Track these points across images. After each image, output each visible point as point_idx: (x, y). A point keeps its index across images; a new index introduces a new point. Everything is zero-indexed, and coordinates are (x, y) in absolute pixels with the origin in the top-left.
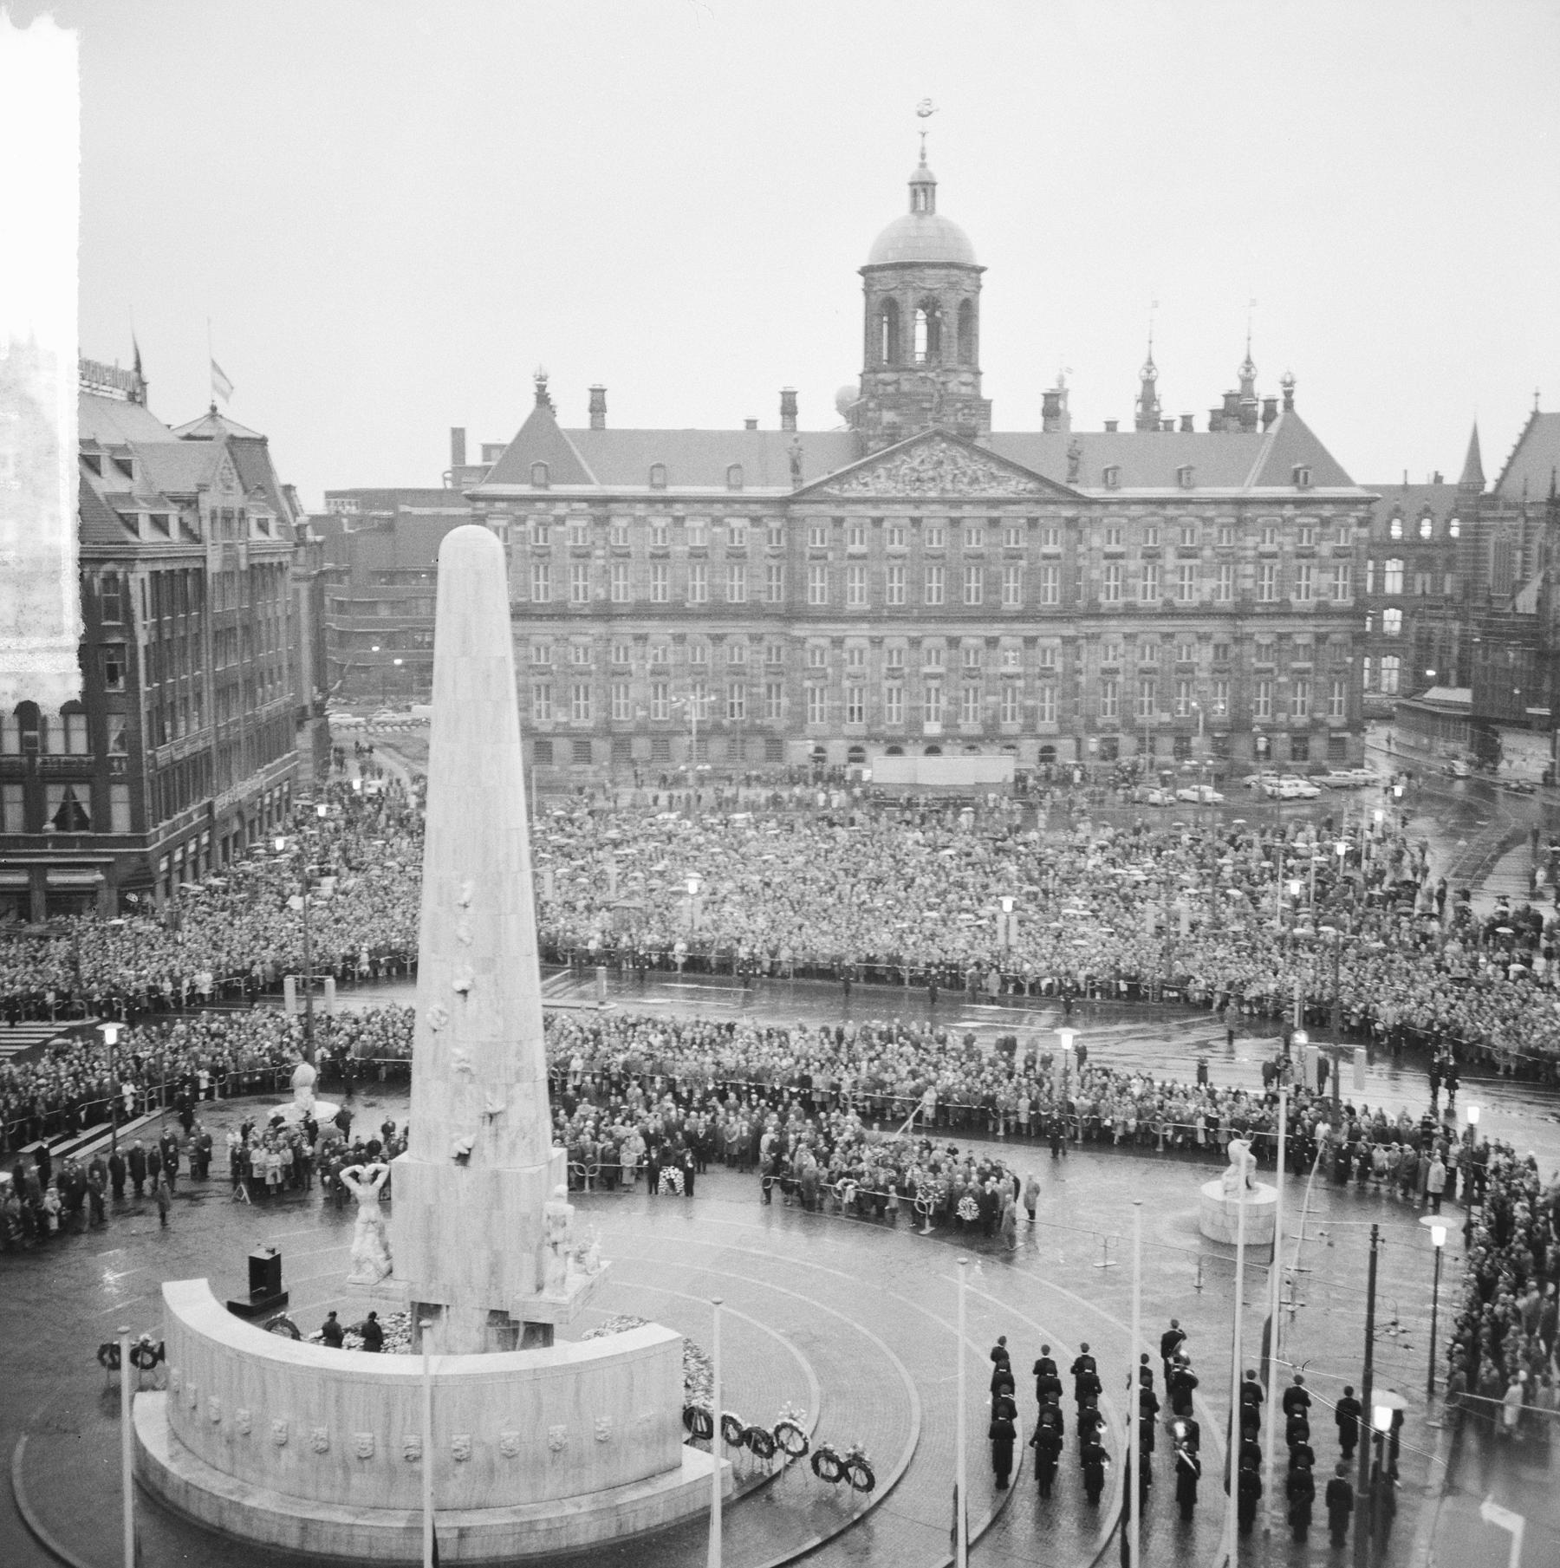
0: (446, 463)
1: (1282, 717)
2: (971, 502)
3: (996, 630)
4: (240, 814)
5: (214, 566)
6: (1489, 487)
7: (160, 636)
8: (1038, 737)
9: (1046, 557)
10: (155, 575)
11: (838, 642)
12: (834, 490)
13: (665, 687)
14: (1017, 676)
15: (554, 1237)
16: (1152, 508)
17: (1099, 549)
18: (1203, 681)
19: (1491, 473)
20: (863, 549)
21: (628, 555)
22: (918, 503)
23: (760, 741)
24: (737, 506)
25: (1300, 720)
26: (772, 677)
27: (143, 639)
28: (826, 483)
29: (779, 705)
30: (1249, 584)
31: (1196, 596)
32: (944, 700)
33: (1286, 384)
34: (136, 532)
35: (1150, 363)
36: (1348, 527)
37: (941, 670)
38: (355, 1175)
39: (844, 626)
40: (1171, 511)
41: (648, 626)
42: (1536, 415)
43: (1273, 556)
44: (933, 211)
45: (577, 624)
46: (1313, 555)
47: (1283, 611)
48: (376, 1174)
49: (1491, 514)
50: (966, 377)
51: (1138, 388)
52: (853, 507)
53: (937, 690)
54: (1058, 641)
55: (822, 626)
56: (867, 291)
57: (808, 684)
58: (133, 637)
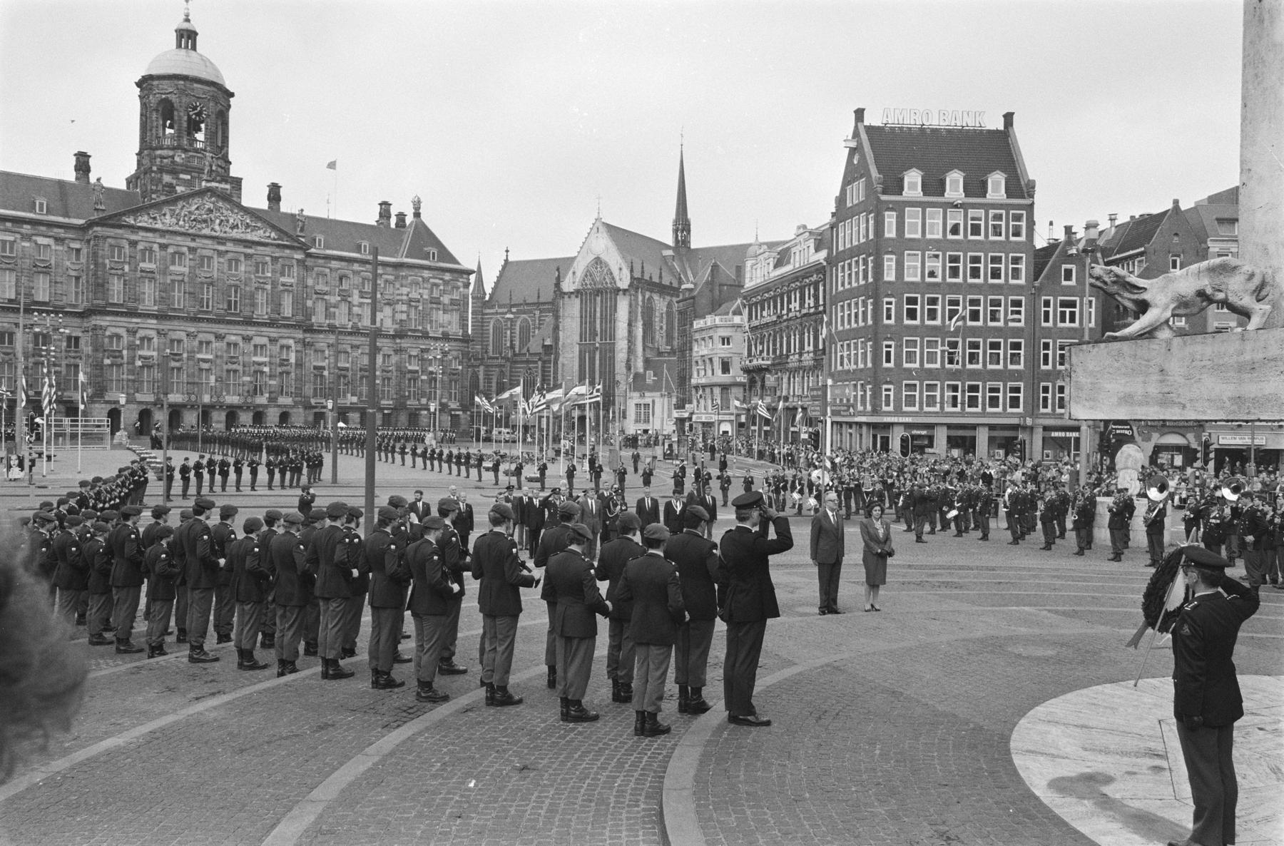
3: (250, 331)
11: (132, 332)
14: (264, 364)
16: (344, 264)
17: (313, 287)
19: (488, 290)
20: (152, 266)
22: (194, 237)
24: (43, 228)
30: (404, 317)
33: (414, 202)
37: (210, 357)
39: (135, 320)
40: (356, 267)
42: (506, 261)
44: (194, 48)
47: (425, 336)
49: (488, 311)
57: (107, 361)
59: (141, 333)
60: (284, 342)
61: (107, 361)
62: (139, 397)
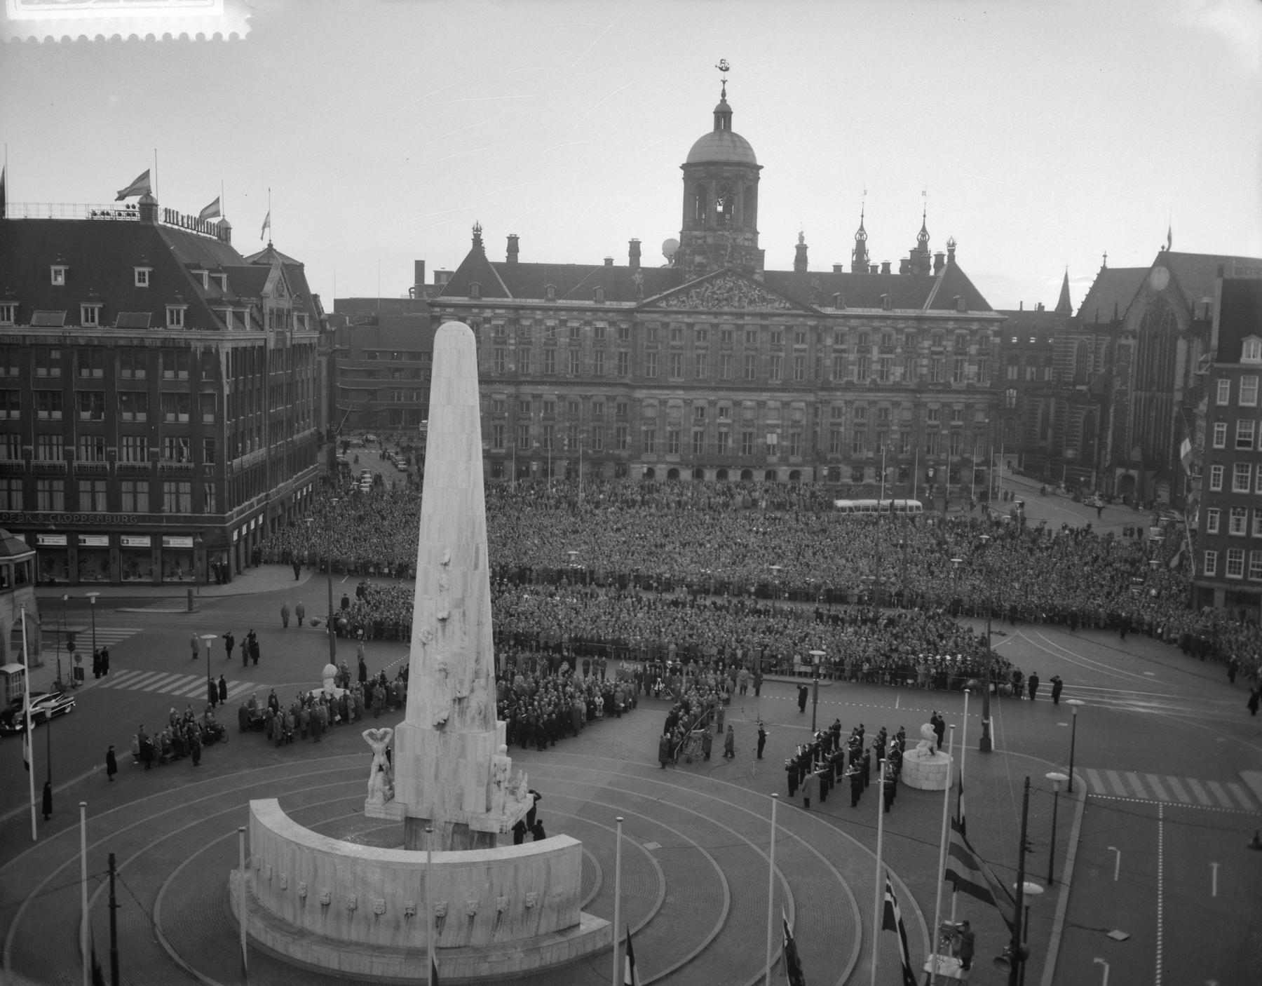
0: (412, 283)
1: (943, 456)
2: (749, 315)
3: (765, 396)
4: (282, 504)
5: (271, 345)
6: (1074, 314)
7: (236, 389)
8: (789, 465)
9: (797, 350)
10: (235, 350)
11: (664, 403)
12: (664, 304)
13: (552, 427)
14: (777, 426)
15: (498, 778)
18: (895, 432)
19: (1076, 303)
21: (530, 343)
22: (716, 315)
23: (612, 464)
24: (600, 314)
25: (956, 458)
26: (620, 424)
27: (227, 391)
28: (658, 300)
29: (624, 441)
30: (925, 370)
31: (892, 378)
32: (730, 441)
33: (949, 245)
34: (225, 323)
35: (862, 228)
36: (987, 337)
37: (729, 421)
38: (371, 735)
40: (876, 324)
41: (540, 389)
42: (1104, 268)
43: (941, 353)
45: (497, 386)
46: (966, 354)
47: (947, 389)
48: (386, 733)
50: (749, 235)
51: (853, 245)
52: (674, 316)
53: (726, 434)
54: (803, 404)
55: (653, 392)
56: (686, 179)
58: (222, 390)
59: (671, 402)
60: (795, 405)
61: (644, 428)
62: (669, 458)
